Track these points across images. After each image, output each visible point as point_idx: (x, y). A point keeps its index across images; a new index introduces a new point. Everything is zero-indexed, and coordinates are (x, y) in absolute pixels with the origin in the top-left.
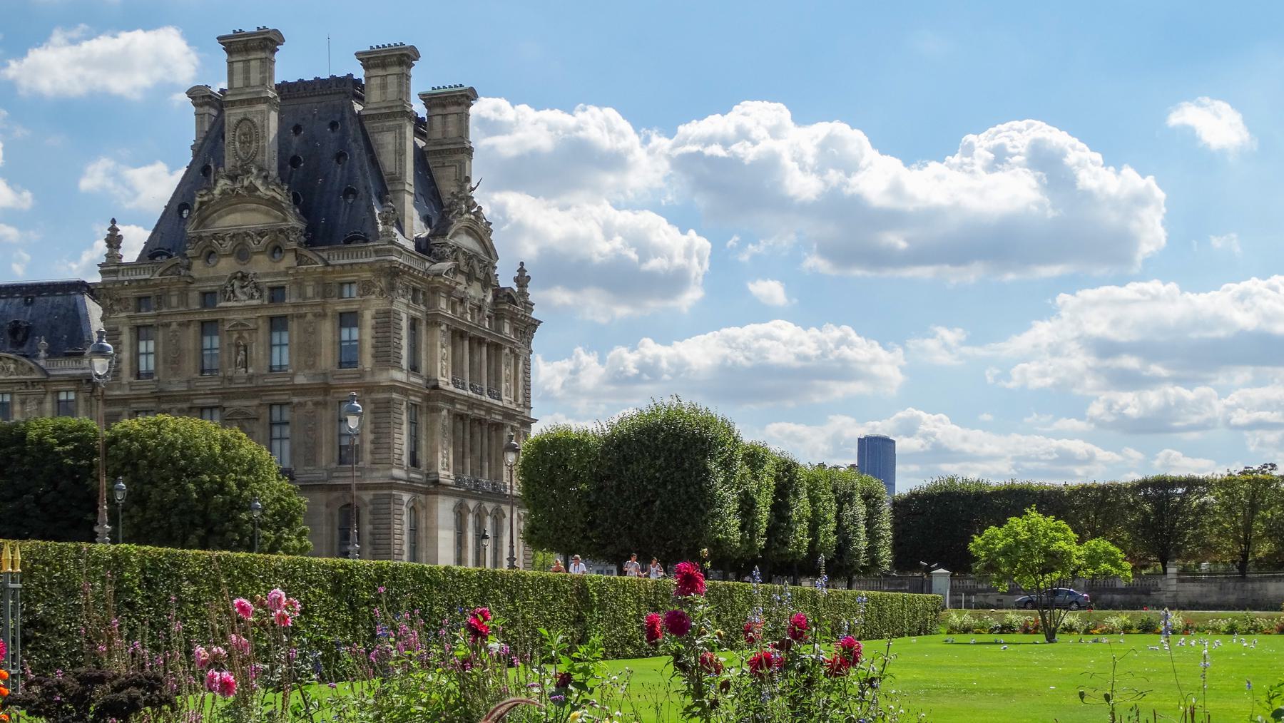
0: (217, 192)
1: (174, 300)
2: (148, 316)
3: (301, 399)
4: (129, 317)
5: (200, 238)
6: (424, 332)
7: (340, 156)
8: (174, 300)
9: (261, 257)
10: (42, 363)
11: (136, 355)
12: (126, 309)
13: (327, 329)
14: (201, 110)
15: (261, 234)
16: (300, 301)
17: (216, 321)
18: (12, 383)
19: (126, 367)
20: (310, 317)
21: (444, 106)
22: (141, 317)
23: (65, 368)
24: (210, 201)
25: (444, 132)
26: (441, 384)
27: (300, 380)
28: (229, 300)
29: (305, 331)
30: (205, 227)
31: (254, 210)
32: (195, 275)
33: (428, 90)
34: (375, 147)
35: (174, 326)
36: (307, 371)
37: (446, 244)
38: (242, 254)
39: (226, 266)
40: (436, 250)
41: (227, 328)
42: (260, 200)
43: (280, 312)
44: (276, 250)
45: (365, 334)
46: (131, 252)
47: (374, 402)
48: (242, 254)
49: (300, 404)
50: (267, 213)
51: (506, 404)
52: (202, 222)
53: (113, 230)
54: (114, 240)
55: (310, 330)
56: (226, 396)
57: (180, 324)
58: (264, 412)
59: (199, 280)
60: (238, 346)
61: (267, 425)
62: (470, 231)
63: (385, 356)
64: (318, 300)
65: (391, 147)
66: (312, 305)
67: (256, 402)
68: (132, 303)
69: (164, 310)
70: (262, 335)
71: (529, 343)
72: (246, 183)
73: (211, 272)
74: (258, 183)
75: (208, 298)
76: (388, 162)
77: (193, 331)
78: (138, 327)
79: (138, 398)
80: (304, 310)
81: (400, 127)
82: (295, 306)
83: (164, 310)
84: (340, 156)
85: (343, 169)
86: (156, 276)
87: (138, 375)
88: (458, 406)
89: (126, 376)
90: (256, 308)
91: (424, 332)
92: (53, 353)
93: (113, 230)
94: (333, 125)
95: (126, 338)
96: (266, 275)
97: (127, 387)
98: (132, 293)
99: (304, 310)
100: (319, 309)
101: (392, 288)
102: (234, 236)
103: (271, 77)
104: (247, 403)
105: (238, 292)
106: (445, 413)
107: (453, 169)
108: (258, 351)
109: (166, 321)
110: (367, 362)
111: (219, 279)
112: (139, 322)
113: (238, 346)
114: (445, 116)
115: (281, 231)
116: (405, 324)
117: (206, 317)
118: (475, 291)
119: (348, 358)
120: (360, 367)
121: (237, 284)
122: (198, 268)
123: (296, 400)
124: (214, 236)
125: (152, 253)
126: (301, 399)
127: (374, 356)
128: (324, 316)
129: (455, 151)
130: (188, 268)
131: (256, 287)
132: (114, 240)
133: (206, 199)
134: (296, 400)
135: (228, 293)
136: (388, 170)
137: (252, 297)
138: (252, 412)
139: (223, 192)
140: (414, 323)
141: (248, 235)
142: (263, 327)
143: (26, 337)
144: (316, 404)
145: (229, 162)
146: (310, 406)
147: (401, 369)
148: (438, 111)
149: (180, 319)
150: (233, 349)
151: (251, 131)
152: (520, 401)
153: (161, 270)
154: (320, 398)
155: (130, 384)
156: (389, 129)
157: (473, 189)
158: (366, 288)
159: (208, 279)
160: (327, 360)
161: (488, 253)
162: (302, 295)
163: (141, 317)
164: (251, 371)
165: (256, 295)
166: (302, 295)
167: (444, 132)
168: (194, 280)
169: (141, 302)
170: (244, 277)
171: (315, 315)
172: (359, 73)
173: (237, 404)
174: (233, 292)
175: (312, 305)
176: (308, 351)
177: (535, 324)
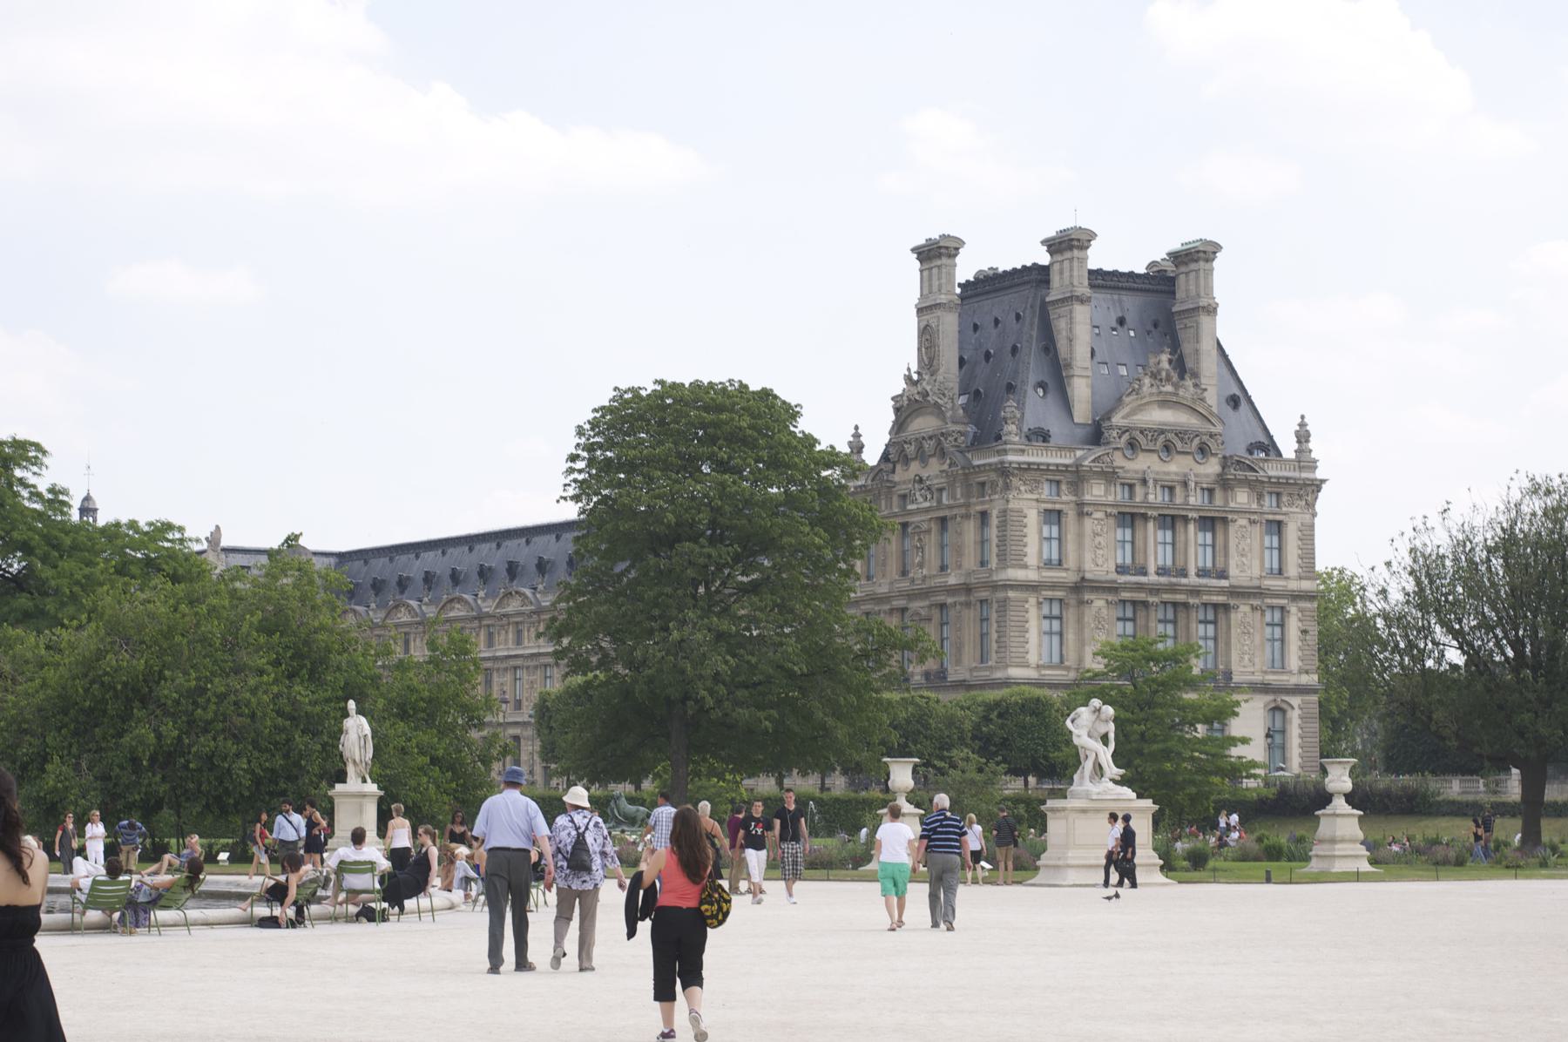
13: (970, 529)
15: (930, 438)
27: (952, 580)
32: (896, 478)
37: (1111, 428)
39: (915, 467)
43: (941, 514)
51: (1234, 582)
56: (911, 596)
58: (936, 613)
62: (1164, 403)
71: (1310, 506)
80: (955, 511)
82: (950, 507)
90: (927, 510)
94: (1018, 317)
99: (955, 511)
100: (963, 511)
103: (951, 276)
116: (1032, 517)
118: (1176, 467)
123: (950, 600)
128: (967, 517)
130: (893, 472)
131: (929, 489)
140: (1053, 516)
142: (934, 527)
147: (1025, 567)
152: (1292, 569)
162: (954, 497)
166: (954, 497)
168: (896, 484)
170: (921, 481)
172: (1044, 258)
177: (1317, 486)
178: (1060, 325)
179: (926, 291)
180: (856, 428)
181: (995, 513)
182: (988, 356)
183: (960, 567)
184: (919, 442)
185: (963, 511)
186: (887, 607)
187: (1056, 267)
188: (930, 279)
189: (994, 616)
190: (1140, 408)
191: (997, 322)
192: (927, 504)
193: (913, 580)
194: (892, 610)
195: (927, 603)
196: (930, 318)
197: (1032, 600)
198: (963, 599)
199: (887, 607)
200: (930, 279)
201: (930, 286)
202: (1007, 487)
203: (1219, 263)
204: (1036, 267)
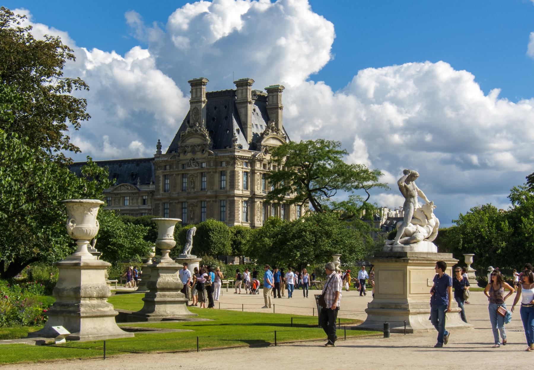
0: (186, 132)
1: (175, 166)
7: (226, 118)
8: (175, 166)
10: (138, 187)
11: (165, 184)
13: (217, 176)
15: (199, 145)
18: (129, 193)
19: (161, 188)
20: (212, 173)
21: (273, 93)
23: (145, 188)
25: (273, 101)
26: (256, 193)
27: (209, 193)
31: (197, 137)
33: (268, 86)
35: (174, 175)
38: (194, 152)
39: (189, 156)
40: (258, 147)
42: (198, 134)
45: (227, 177)
47: (230, 201)
48: (194, 152)
49: (208, 201)
50: (201, 138)
52: (183, 141)
54: (159, 147)
57: (176, 175)
59: (182, 160)
60: (192, 182)
64: (214, 167)
65: (244, 113)
67: (196, 200)
69: (172, 170)
70: (199, 178)
72: (194, 129)
77: (180, 177)
78: (165, 175)
87: (165, 191)
89: (161, 191)
90: (197, 170)
92: (142, 183)
93: (159, 143)
94: (226, 107)
95: (161, 179)
96: (200, 159)
98: (163, 164)
99: (210, 170)
100: (214, 170)
104: (194, 201)
106: (258, 202)
108: (198, 184)
111: (187, 160)
112: (165, 173)
113: (192, 182)
114: (273, 96)
115: (204, 145)
117: (183, 172)
121: (192, 161)
123: (207, 200)
124: (186, 146)
125: (170, 151)
127: (230, 186)
128: (216, 172)
130: (179, 156)
132: (159, 147)
134: (207, 200)
135: (189, 165)
137: (196, 166)
139: (188, 132)
142: (199, 175)
143: (135, 178)
144: (213, 201)
147: (239, 190)
148: (271, 94)
149: (176, 173)
154: (214, 199)
155: (162, 194)
156: (243, 107)
159: (184, 160)
167: (273, 101)
168: (180, 160)
170: (194, 159)
172: (235, 88)
173: (191, 201)
176: (211, 183)
178: (242, 110)
179: (194, 96)
181: (228, 172)
182: (214, 119)
184: (193, 146)
186: (177, 201)
187: (240, 91)
188: (196, 92)
190: (267, 140)
191: (215, 108)
192: (197, 168)
193: (189, 193)
194: (178, 202)
196: (194, 105)
197: (241, 201)
198: (214, 199)
199: (177, 201)
200: (196, 92)
201: (196, 94)
202: (234, 163)
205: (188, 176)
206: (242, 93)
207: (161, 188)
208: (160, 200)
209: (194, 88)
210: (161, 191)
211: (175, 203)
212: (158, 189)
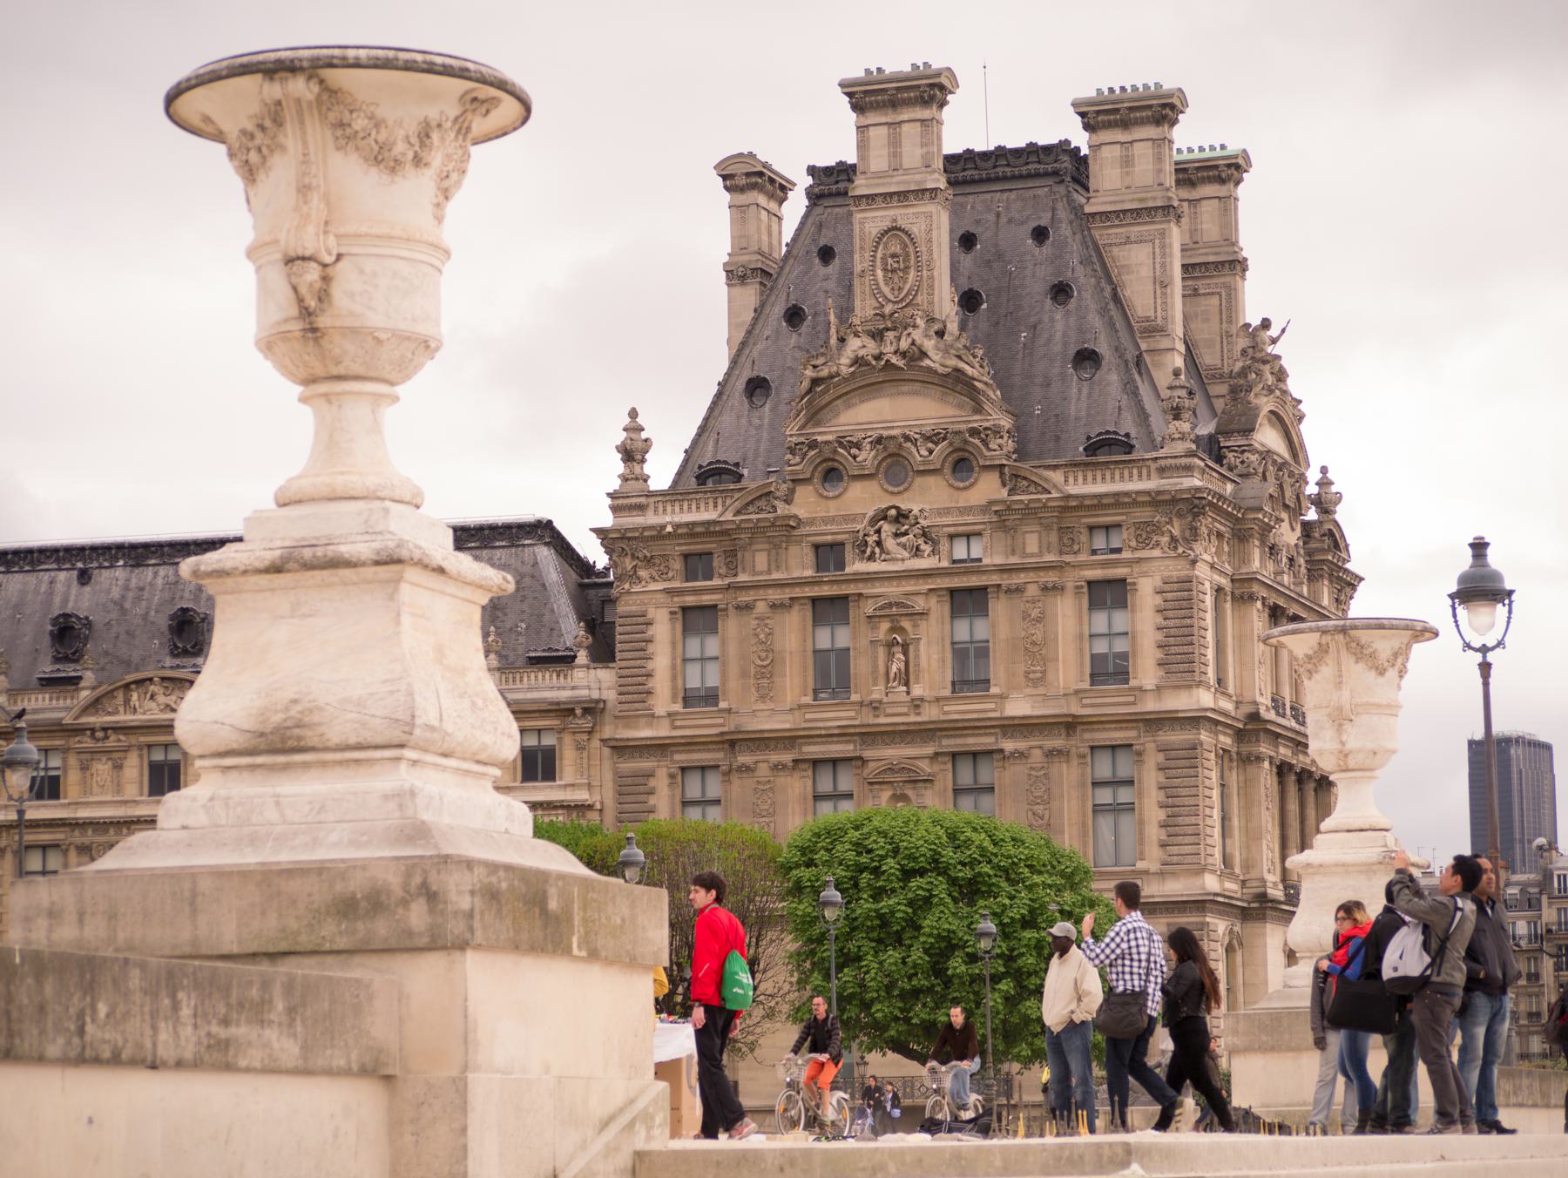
1: (761, 560)
2: (706, 591)
3: (1021, 745)
4: (668, 591)
5: (813, 445)
6: (1229, 612)
9: (931, 480)
12: (663, 576)
13: (1067, 614)
14: (743, 199)
15: (933, 438)
16: (1014, 560)
17: (845, 598)
22: (695, 591)
24: (831, 377)
27: (1019, 707)
28: (871, 558)
29: (1026, 616)
30: (817, 424)
34: (1114, 273)
36: (1029, 691)
37: (1250, 449)
41: (870, 611)
44: (962, 465)
45: (1144, 619)
46: (661, 470)
49: (1021, 755)
53: (634, 428)
55: (1035, 613)
56: (870, 736)
59: (812, 521)
60: (891, 644)
61: (950, 794)
63: (1180, 660)
65: (1146, 272)
66: (1038, 568)
68: (677, 565)
73: (833, 508)
74: (929, 345)
75: (829, 554)
76: (1140, 297)
78: (685, 609)
79: (690, 744)
81: (1163, 234)
82: (1004, 570)
83: (743, 578)
84: (1061, 292)
85: (1068, 313)
86: (729, 516)
88: (1282, 750)
91: (1229, 612)
93: (634, 428)
94: (1040, 234)
96: (946, 511)
97: (666, 722)
101: (1194, 535)
102: (879, 440)
105: (890, 543)
107: (1215, 300)
109: (744, 598)
110: (1146, 673)
111: (848, 518)
112: (690, 600)
113: (894, 643)
115: (974, 432)
117: (826, 591)
119: (1110, 670)
120: (1133, 683)
121: (887, 528)
122: (806, 504)
123: (1009, 745)
125: (706, 473)
126: (1021, 745)
129: (1219, 265)
133: (825, 373)
136: (1140, 313)
137: (917, 552)
138: (925, 767)
141: (907, 438)
144: (1051, 754)
145: (864, 308)
146: (1037, 753)
150: (881, 652)
151: (901, 249)
153: (738, 505)
157: (1274, 341)
158: (1146, 534)
160: (1068, 672)
161: (1295, 455)
163: (695, 591)
164: (917, 691)
165: (927, 548)
169: (697, 565)
170: (902, 516)
171: (1045, 589)
174: (879, 543)
175: (1038, 568)
180: (633, 414)
183: (1040, 681)
185: (1051, 578)
186: (787, 757)
188: (895, 143)
189: (1151, 778)
193: (875, 707)
195: (929, 750)
198: (1058, 742)
199: (787, 757)
200: (895, 143)
203: (1248, 191)
204: (1063, 148)
205: (869, 608)
206: (1127, 162)
207: (661, 684)
208: (659, 748)
209: (872, 118)
210: (663, 701)
211: (776, 767)
212: (636, 690)
